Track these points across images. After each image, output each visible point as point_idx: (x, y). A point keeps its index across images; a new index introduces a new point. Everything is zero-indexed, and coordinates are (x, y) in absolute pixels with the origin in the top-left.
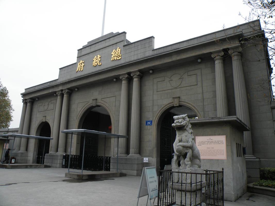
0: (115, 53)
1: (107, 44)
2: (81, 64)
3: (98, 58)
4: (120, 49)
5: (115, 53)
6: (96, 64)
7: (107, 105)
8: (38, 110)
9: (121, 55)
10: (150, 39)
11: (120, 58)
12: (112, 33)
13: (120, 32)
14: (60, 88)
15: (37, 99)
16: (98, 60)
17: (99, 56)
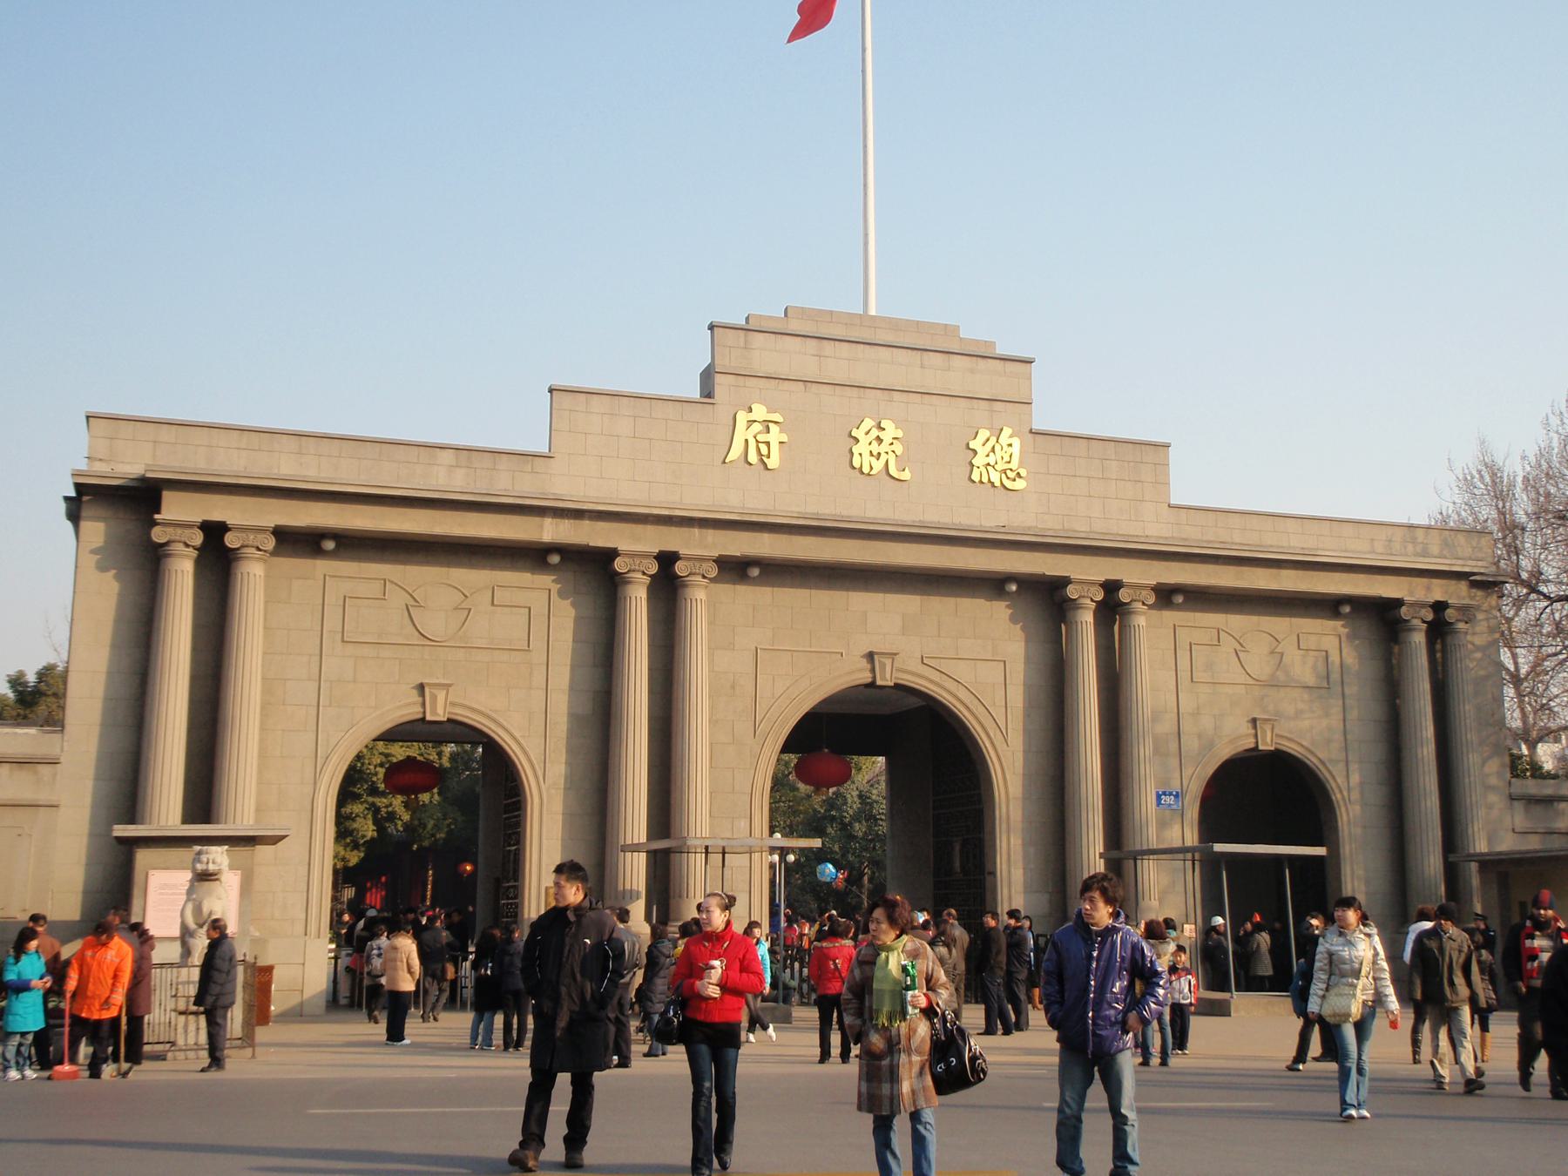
0: (993, 450)
1: (932, 382)
2: (757, 427)
3: (887, 436)
4: (1016, 442)
5: (993, 450)
6: (878, 466)
7: (963, 694)
8: (333, 621)
9: (1023, 472)
10: (1149, 454)
11: (1020, 484)
12: (950, 330)
13: (1000, 350)
14: (653, 541)
15: (329, 545)
16: (884, 447)
17: (891, 430)
